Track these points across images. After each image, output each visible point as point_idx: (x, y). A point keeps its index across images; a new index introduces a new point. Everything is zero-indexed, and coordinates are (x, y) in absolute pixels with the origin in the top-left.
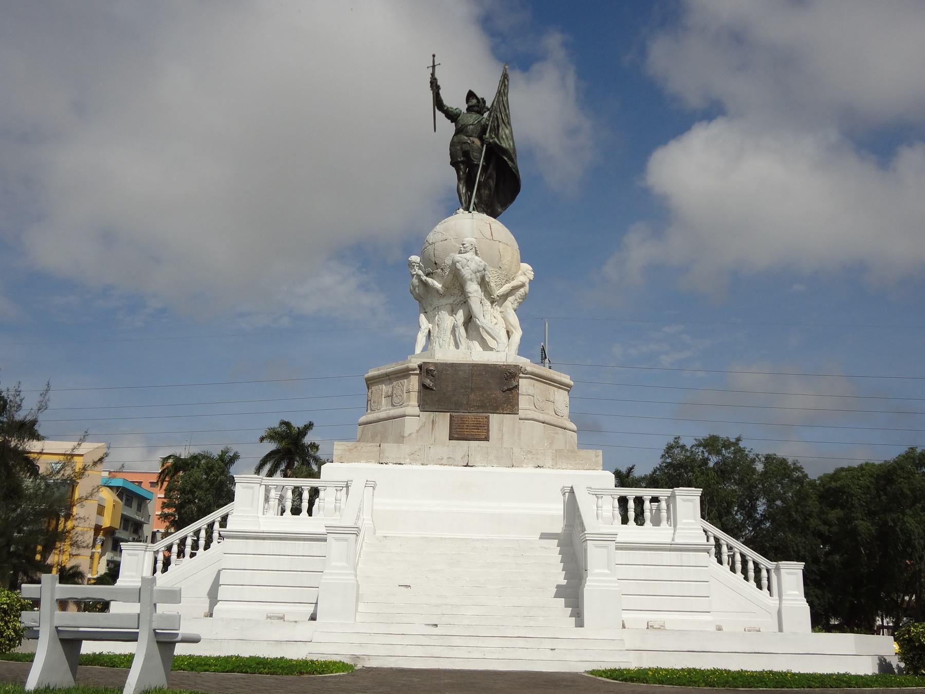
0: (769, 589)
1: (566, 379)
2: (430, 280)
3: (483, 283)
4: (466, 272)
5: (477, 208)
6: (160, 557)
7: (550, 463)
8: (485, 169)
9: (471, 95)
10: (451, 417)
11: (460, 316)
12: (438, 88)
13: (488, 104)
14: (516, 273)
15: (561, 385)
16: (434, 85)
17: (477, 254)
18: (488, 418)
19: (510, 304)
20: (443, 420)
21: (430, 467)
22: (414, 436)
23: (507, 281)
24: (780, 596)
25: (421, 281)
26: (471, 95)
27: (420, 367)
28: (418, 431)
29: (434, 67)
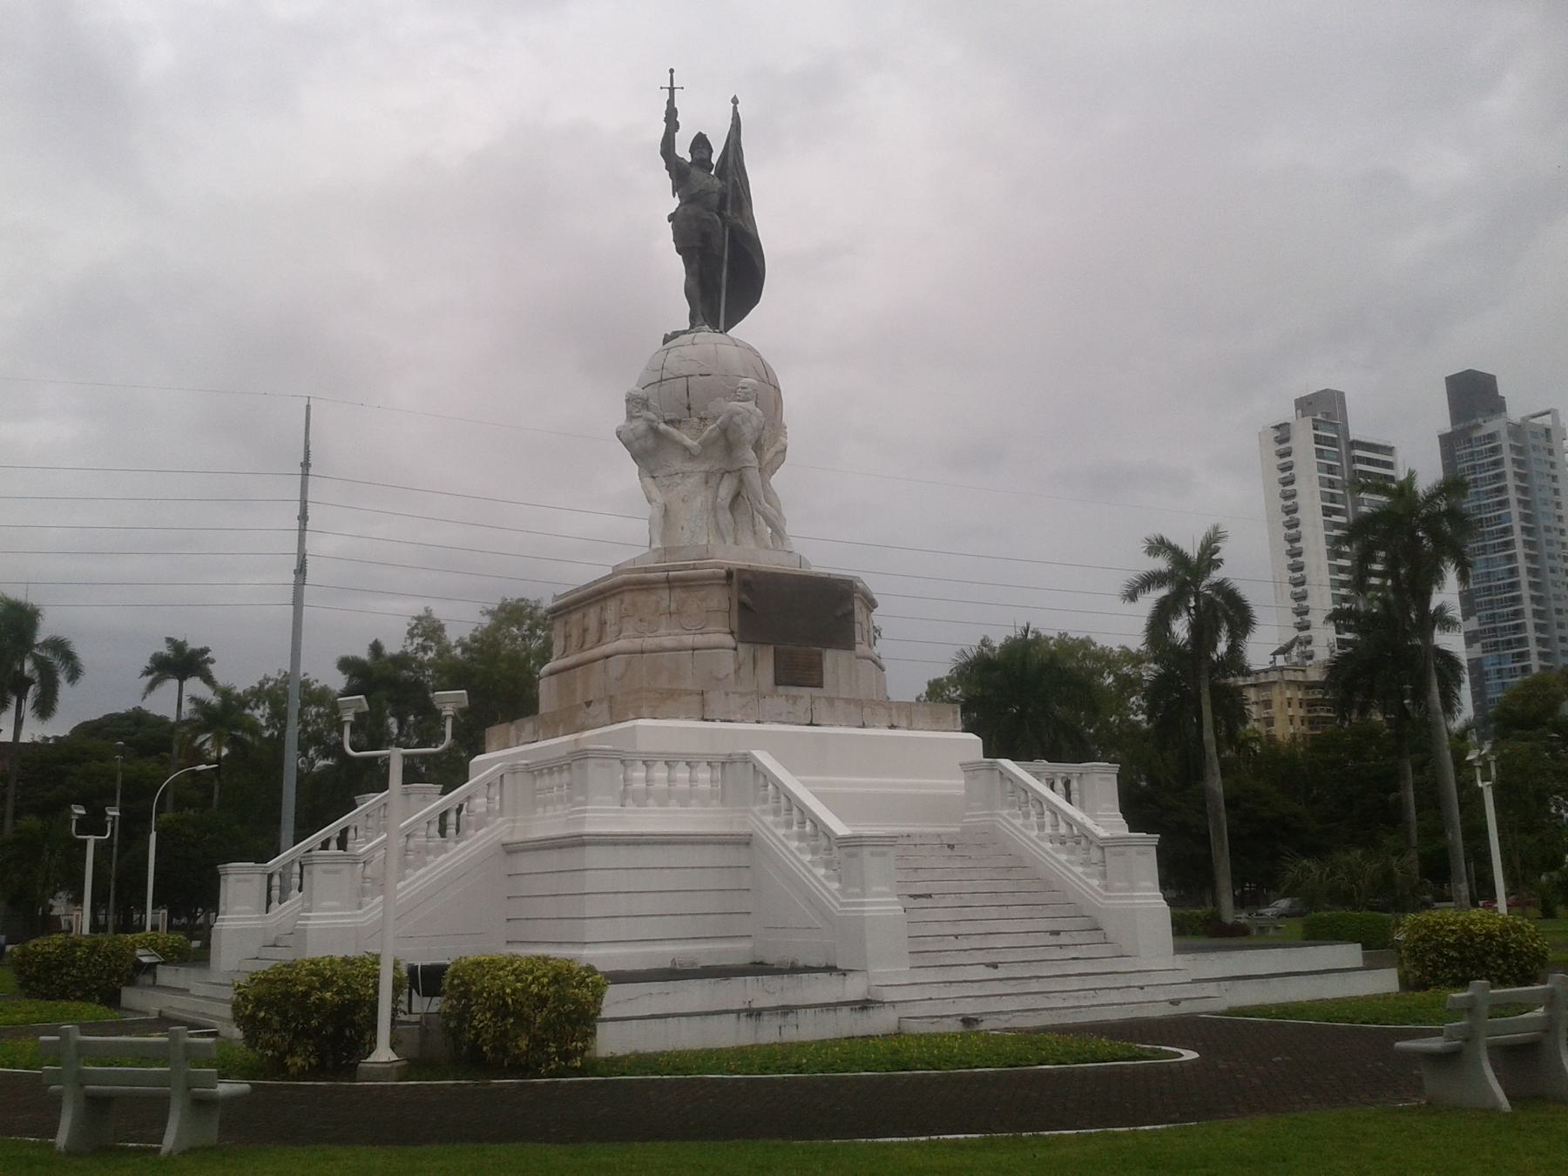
3: (758, 447)
4: (748, 432)
7: (904, 723)
11: (726, 490)
12: (677, 126)
18: (820, 655)
25: (654, 431)
27: (730, 574)
29: (672, 89)
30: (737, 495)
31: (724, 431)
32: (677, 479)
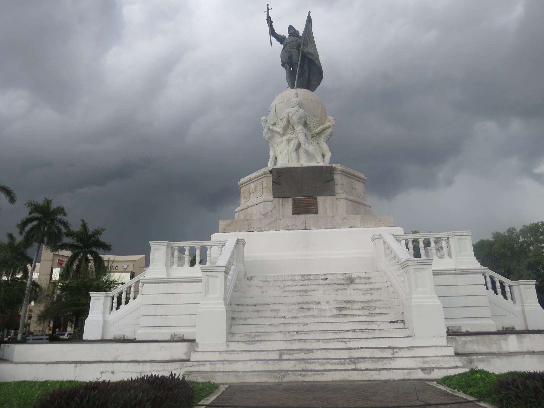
0: (512, 299)
1: (362, 176)
2: (274, 128)
3: (305, 125)
5: (298, 87)
6: (115, 300)
8: (302, 66)
9: (291, 28)
10: (294, 200)
13: (301, 34)
14: (325, 120)
15: (359, 179)
16: (270, 21)
17: (300, 108)
18: (316, 199)
19: (322, 140)
20: (289, 205)
21: (281, 232)
22: (270, 214)
23: (320, 125)
24: (522, 302)
26: (291, 28)
28: (271, 211)
29: (268, 11)
30: (299, 146)
31: (288, 121)
32: (279, 146)
